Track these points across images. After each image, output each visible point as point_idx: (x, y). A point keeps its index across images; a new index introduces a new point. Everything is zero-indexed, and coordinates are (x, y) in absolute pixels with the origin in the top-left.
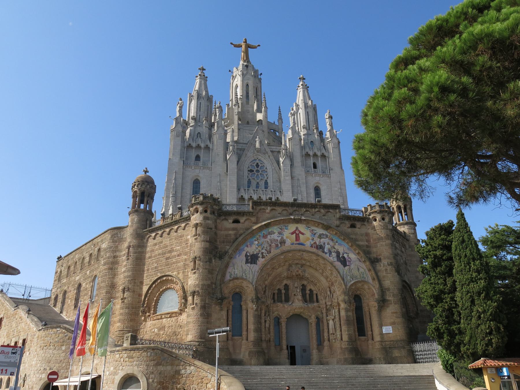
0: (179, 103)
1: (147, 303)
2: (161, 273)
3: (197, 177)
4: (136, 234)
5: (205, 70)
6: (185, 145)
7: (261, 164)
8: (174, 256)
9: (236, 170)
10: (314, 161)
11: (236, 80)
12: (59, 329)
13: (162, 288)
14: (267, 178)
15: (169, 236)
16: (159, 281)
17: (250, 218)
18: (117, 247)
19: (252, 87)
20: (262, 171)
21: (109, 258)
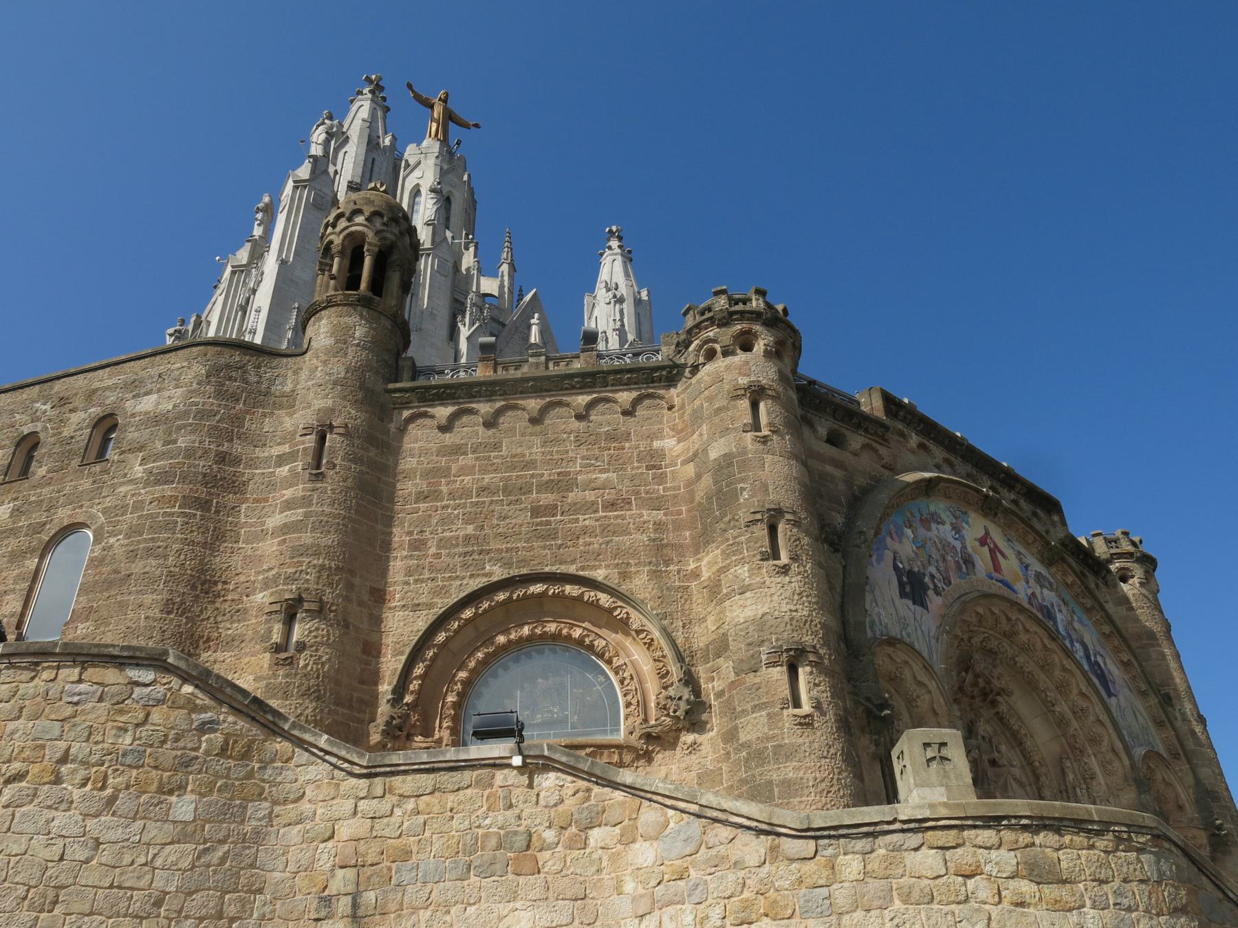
0: (323, 123)
1: (419, 692)
2: (508, 565)
4: (361, 388)
8: (578, 508)
12: (147, 676)
13: (506, 631)
15: (538, 428)
16: (501, 597)
17: (874, 444)
18: (238, 420)
21: (189, 453)
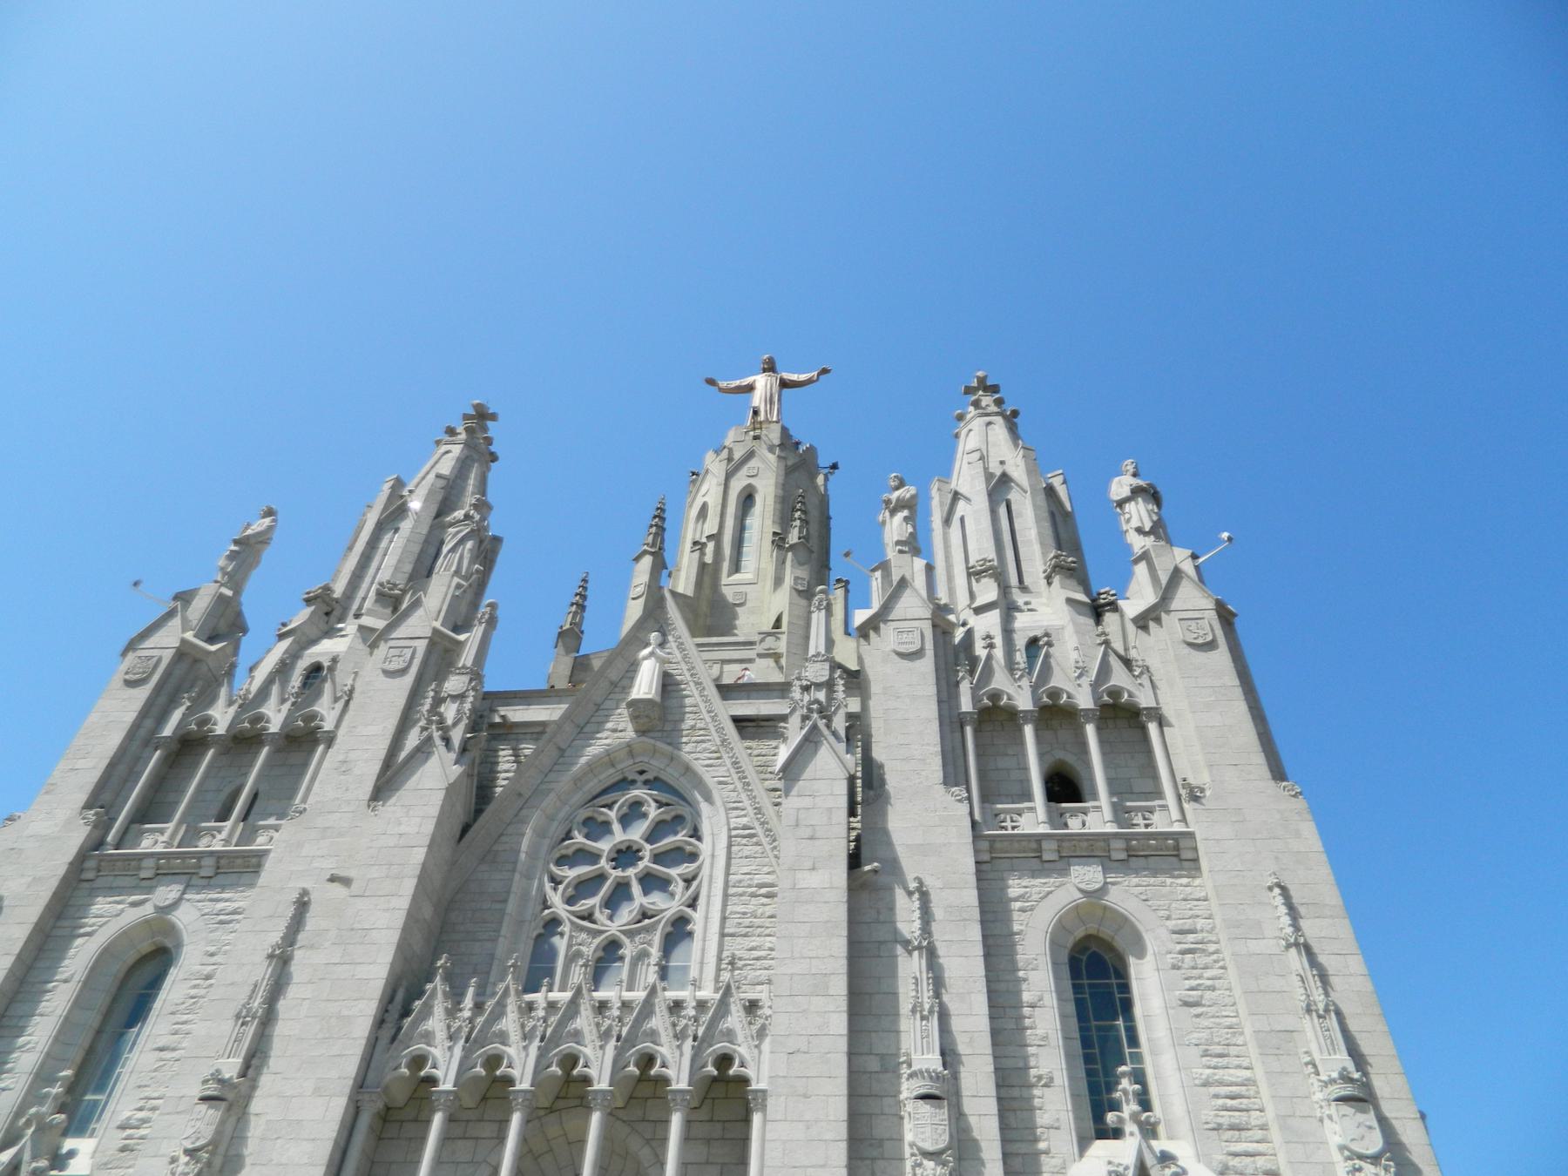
3: (159, 939)
5: (493, 417)
6: (168, 730)
7: (660, 804)
9: (419, 855)
10: (1060, 755)
11: (704, 489)
14: (692, 904)
19: (770, 501)
20: (658, 858)
